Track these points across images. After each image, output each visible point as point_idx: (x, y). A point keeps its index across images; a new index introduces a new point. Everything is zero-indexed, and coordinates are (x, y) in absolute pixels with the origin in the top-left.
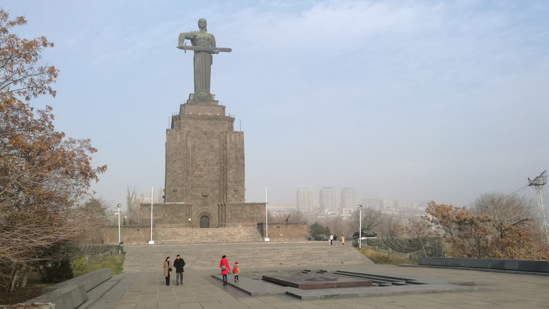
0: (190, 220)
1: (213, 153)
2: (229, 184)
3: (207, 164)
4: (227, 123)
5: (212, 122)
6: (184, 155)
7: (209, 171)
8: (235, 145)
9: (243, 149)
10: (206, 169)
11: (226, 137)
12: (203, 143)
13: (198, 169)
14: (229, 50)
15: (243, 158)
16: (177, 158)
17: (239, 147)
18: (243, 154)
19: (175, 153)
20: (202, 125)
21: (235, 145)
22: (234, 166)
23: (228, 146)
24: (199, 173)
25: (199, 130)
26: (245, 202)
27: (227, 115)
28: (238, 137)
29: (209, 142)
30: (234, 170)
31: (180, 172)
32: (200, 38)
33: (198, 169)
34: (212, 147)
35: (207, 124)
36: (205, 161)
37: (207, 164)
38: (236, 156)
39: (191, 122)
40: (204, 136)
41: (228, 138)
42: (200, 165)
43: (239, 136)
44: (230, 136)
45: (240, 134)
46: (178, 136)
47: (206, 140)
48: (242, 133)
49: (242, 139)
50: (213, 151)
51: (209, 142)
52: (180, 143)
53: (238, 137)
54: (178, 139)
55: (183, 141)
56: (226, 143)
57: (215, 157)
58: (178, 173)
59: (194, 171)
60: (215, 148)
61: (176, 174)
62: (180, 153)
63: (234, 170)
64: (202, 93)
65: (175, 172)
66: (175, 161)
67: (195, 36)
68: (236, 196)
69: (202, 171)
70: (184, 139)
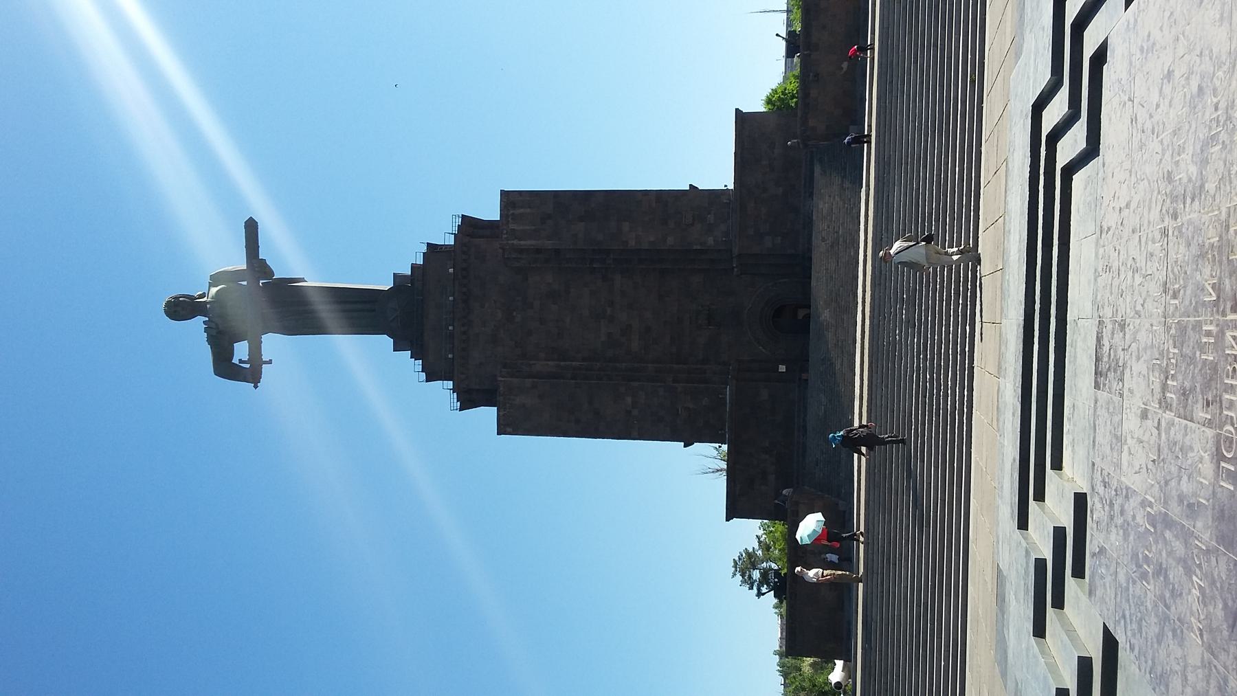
0: (782, 368)
2: (670, 240)
3: (609, 310)
11: (521, 251)
14: (251, 227)
23: (549, 244)
26: (731, 186)
27: (451, 241)
30: (626, 226)
31: (629, 400)
41: (524, 243)
45: (509, 199)
48: (505, 194)
56: (538, 251)
61: (635, 412)
63: (626, 226)
68: (711, 218)
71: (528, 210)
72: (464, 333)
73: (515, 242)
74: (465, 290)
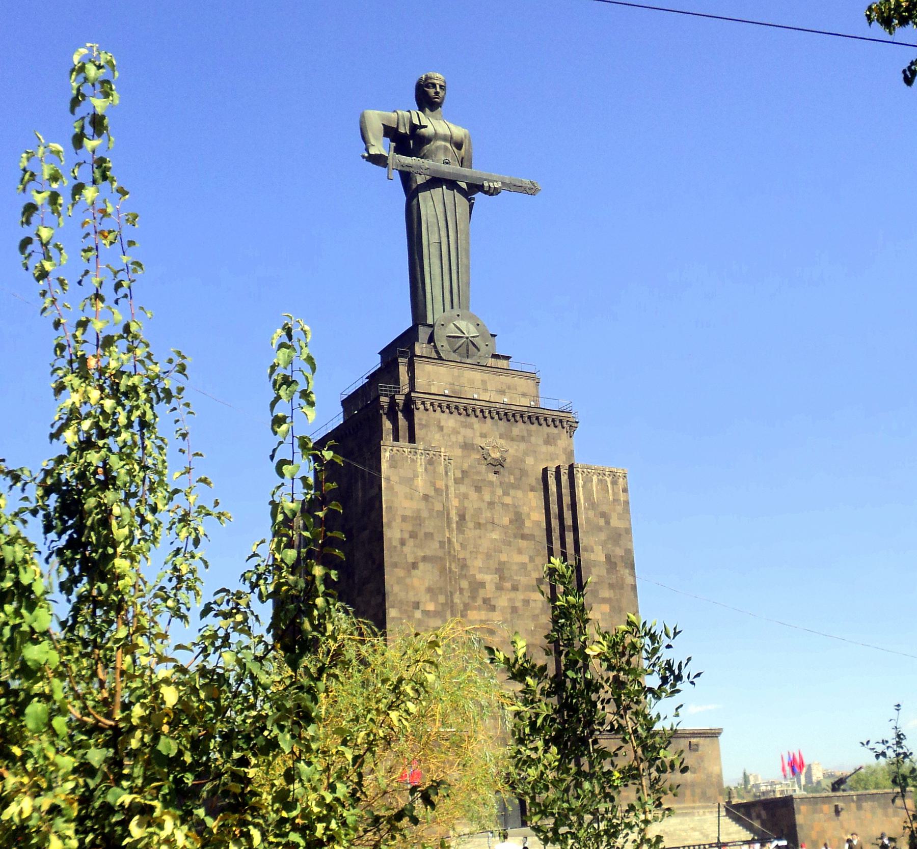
1: (523, 544)
5: (519, 429)
6: (442, 543)
7: (514, 610)
8: (603, 515)
9: (628, 531)
10: (502, 602)
12: (491, 504)
13: (479, 602)
15: (632, 567)
16: (421, 554)
17: (615, 522)
18: (629, 552)
19: (413, 535)
20: (483, 436)
21: (603, 515)
22: (606, 593)
24: (483, 615)
29: (508, 500)
30: (606, 608)
31: (431, 607)
32: (436, 136)
33: (479, 602)
34: (518, 519)
35: (501, 436)
36: (501, 570)
37: (508, 585)
38: (608, 557)
39: (450, 421)
40: (493, 478)
42: (482, 585)
43: (614, 483)
46: (421, 470)
47: (499, 492)
49: (622, 497)
50: (523, 537)
51: (508, 500)
52: (426, 497)
54: (420, 482)
57: (532, 559)
58: (426, 613)
59: (466, 606)
60: (528, 524)
61: (418, 614)
62: (429, 536)
63: (606, 608)
64: (462, 324)
65: (417, 605)
66: (414, 566)
67: (414, 128)
69: (493, 608)
70: (441, 484)
71: (611, 498)
72: (474, 410)
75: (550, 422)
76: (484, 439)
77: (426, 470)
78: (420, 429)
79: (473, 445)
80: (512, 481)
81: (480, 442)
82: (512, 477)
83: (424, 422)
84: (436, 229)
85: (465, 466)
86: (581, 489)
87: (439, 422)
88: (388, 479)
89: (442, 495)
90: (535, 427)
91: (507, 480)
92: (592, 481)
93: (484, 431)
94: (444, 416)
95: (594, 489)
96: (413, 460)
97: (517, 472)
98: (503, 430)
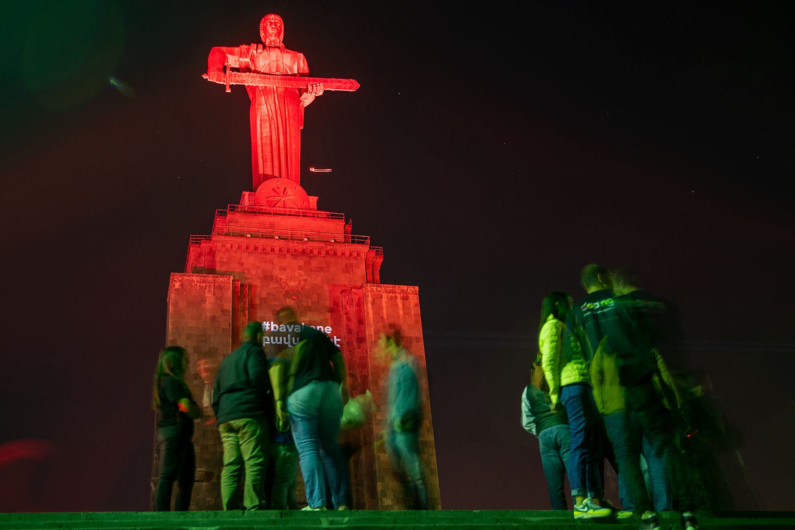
4: (363, 266)
11: (360, 304)
20: (283, 269)
25: (273, 285)
28: (399, 301)
35: (300, 268)
44: (377, 298)
52: (213, 318)
53: (399, 301)
55: (224, 312)
56: (361, 321)
71: (401, 312)
73: (370, 299)
74: (316, 252)
75: (347, 254)
76: (283, 272)
77: (214, 294)
78: (221, 266)
79: (272, 277)
80: (310, 304)
81: (277, 273)
82: (310, 301)
83: (225, 260)
84: (268, 124)
85: (264, 295)
86: (370, 305)
87: (241, 259)
88: (176, 304)
89: (229, 315)
90: (333, 259)
91: (305, 304)
92: (381, 297)
93: (284, 265)
94: (246, 254)
95: (384, 304)
96: (201, 287)
97: (315, 297)
98: (301, 263)
